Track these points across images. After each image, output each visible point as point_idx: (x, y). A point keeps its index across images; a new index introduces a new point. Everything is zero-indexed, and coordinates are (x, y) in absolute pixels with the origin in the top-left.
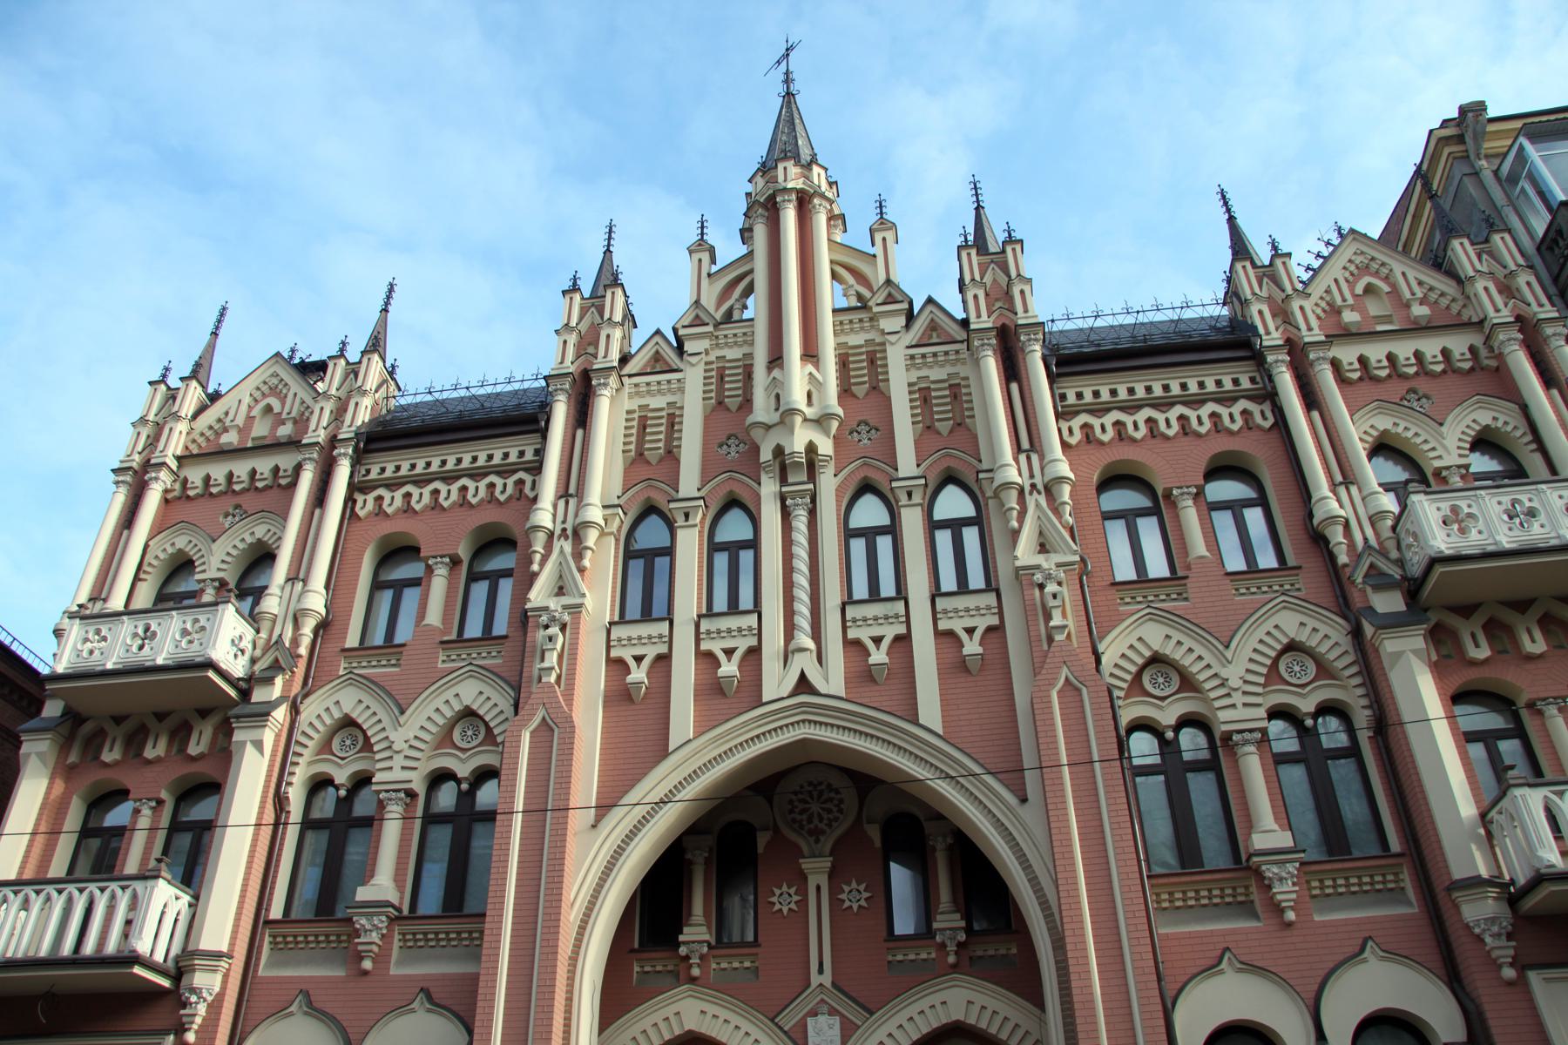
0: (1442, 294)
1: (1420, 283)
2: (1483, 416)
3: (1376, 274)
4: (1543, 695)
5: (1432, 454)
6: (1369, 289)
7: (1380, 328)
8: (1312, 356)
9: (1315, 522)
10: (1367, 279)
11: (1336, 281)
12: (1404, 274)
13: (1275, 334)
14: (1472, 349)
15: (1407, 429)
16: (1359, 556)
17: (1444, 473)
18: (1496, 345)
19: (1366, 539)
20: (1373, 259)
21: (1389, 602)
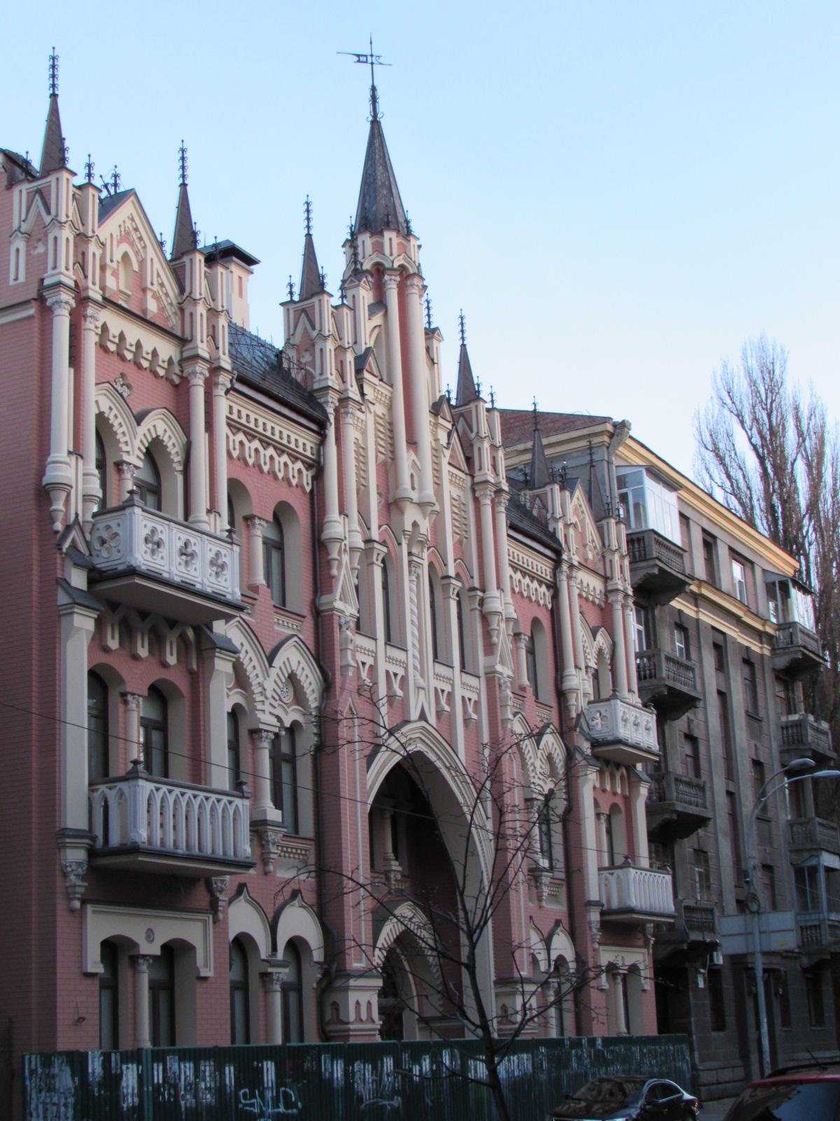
0: (167, 295)
1: (159, 275)
2: (159, 425)
3: (132, 244)
4: (134, 691)
5: (125, 448)
6: (125, 256)
7: (121, 302)
8: (90, 311)
9: (45, 480)
10: (125, 247)
11: (112, 235)
12: (152, 260)
13: (70, 273)
14: (170, 361)
15: (120, 422)
16: (68, 528)
17: (125, 467)
18: (188, 370)
19: (77, 515)
20: (136, 229)
21: (78, 579)
